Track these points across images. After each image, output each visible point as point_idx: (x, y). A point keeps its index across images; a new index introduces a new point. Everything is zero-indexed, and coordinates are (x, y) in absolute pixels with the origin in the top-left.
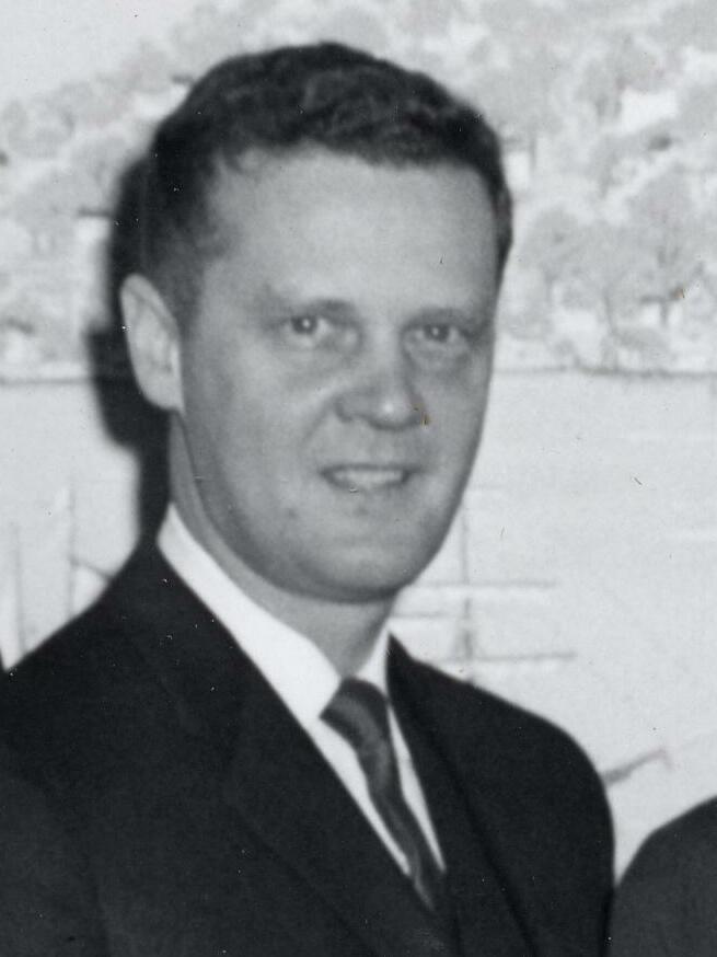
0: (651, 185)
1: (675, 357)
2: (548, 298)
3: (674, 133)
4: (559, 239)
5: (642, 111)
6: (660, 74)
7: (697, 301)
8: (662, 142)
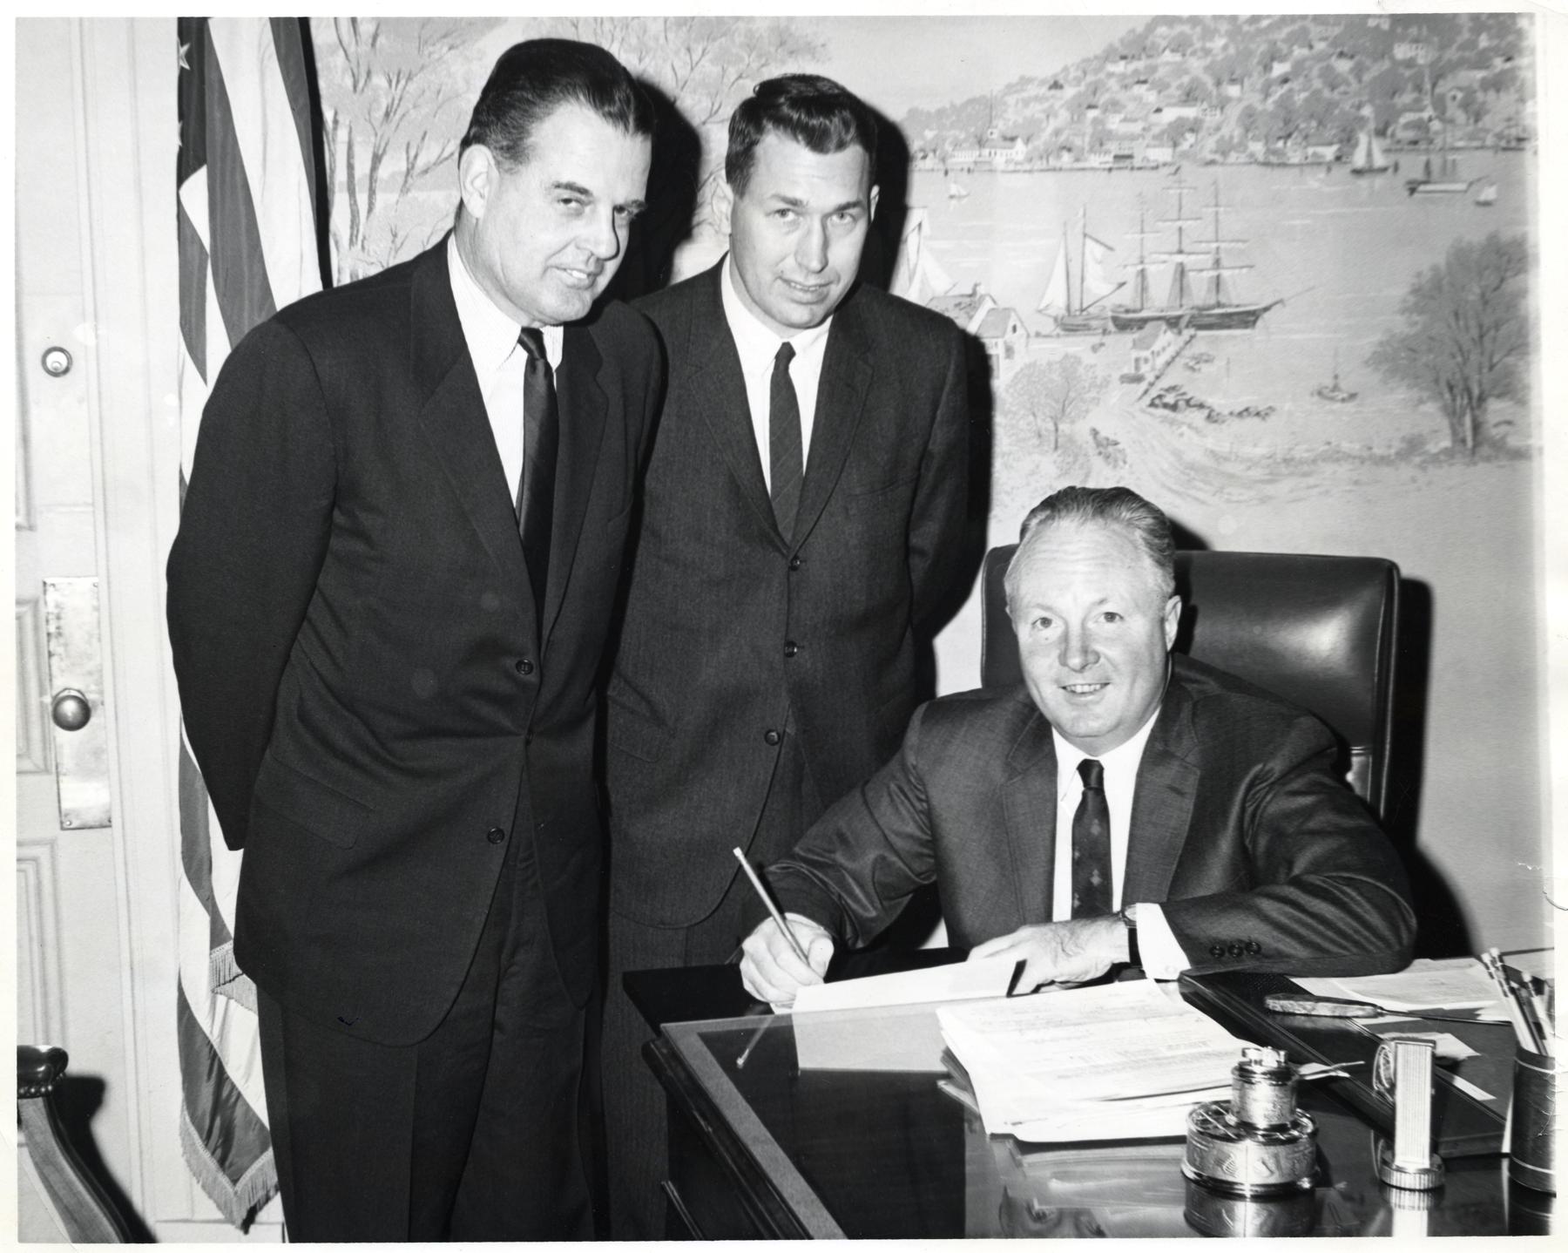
0: (1282, 96)
1: (1289, 159)
2: (1246, 137)
3: (1290, 77)
4: (1250, 116)
5: (1279, 69)
6: (1286, 55)
7: (1296, 138)
8: (1285, 80)
